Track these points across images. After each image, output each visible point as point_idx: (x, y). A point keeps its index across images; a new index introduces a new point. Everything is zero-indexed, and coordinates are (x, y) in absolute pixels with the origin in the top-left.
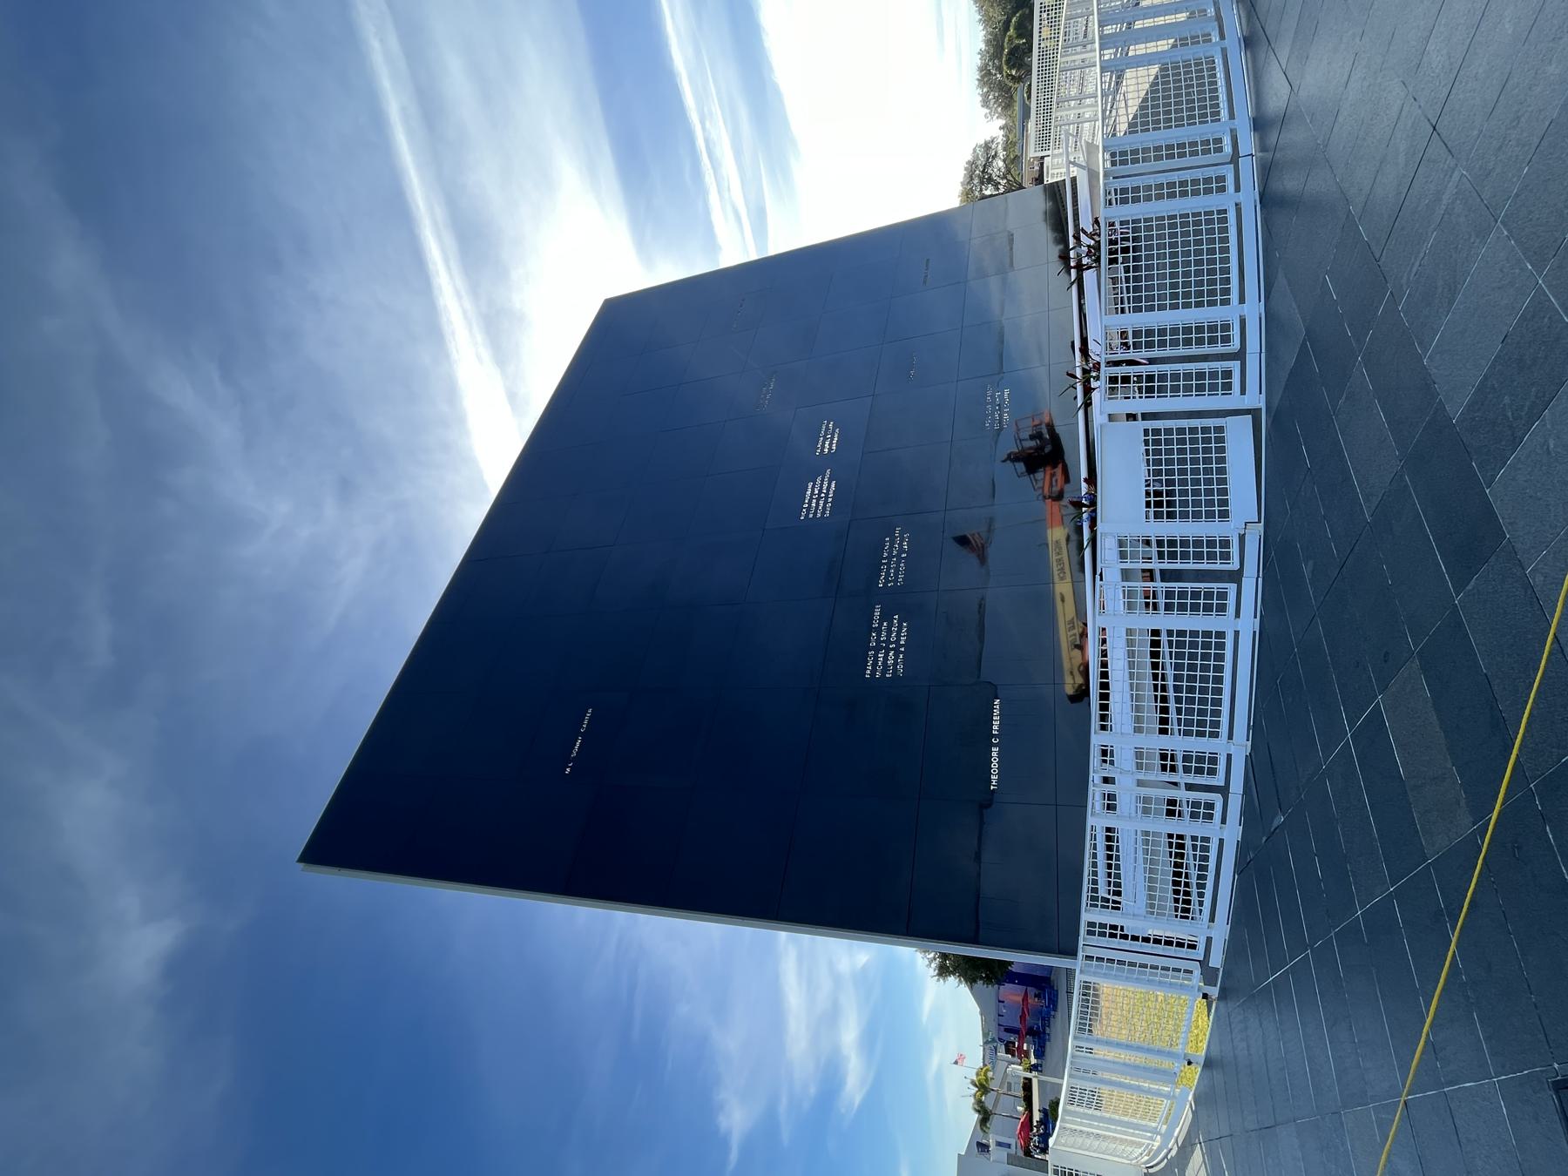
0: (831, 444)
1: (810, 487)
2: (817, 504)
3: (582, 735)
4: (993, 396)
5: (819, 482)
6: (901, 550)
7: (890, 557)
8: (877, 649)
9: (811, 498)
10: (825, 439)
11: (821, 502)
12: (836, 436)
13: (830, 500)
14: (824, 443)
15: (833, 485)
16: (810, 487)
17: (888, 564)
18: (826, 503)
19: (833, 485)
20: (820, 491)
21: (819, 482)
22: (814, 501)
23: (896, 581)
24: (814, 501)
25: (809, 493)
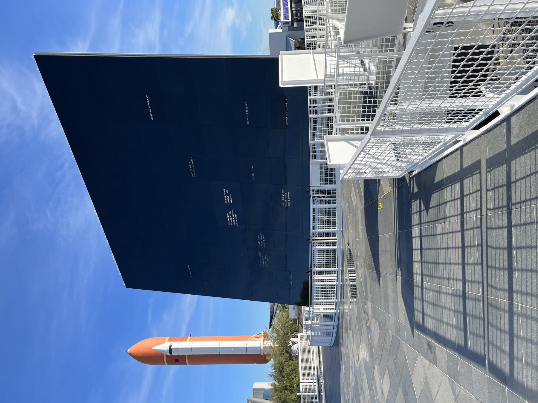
0: (230, 200)
1: (228, 215)
2: (232, 216)
3: (190, 270)
4: (284, 194)
5: (230, 213)
6: (263, 239)
7: (260, 241)
8: (262, 261)
9: (230, 220)
10: (227, 198)
11: (234, 221)
12: (231, 197)
13: (236, 220)
14: (227, 199)
15: (236, 216)
16: (228, 215)
17: (260, 242)
18: (235, 221)
19: (236, 216)
20: (232, 216)
21: (230, 213)
22: (231, 220)
23: (263, 246)
24: (231, 220)
25: (228, 217)
